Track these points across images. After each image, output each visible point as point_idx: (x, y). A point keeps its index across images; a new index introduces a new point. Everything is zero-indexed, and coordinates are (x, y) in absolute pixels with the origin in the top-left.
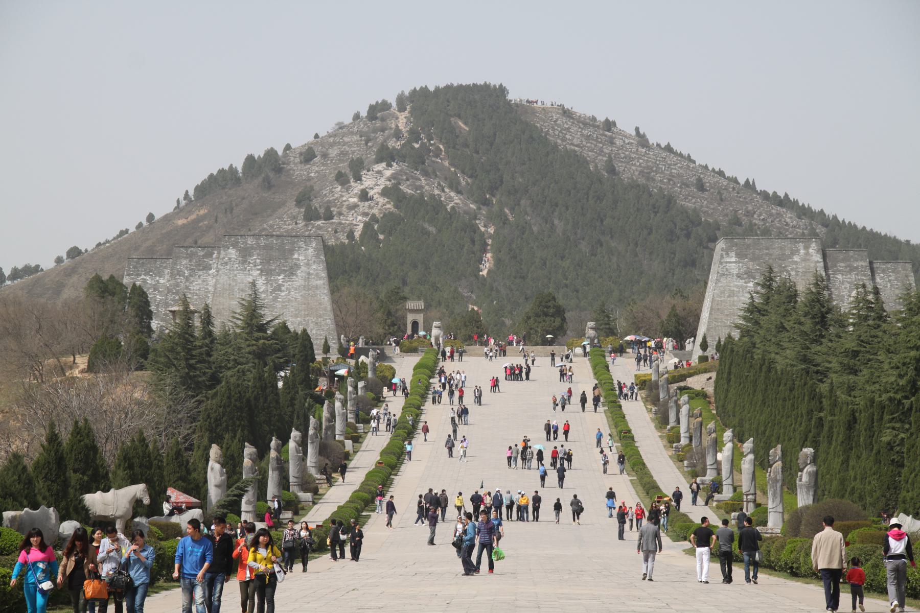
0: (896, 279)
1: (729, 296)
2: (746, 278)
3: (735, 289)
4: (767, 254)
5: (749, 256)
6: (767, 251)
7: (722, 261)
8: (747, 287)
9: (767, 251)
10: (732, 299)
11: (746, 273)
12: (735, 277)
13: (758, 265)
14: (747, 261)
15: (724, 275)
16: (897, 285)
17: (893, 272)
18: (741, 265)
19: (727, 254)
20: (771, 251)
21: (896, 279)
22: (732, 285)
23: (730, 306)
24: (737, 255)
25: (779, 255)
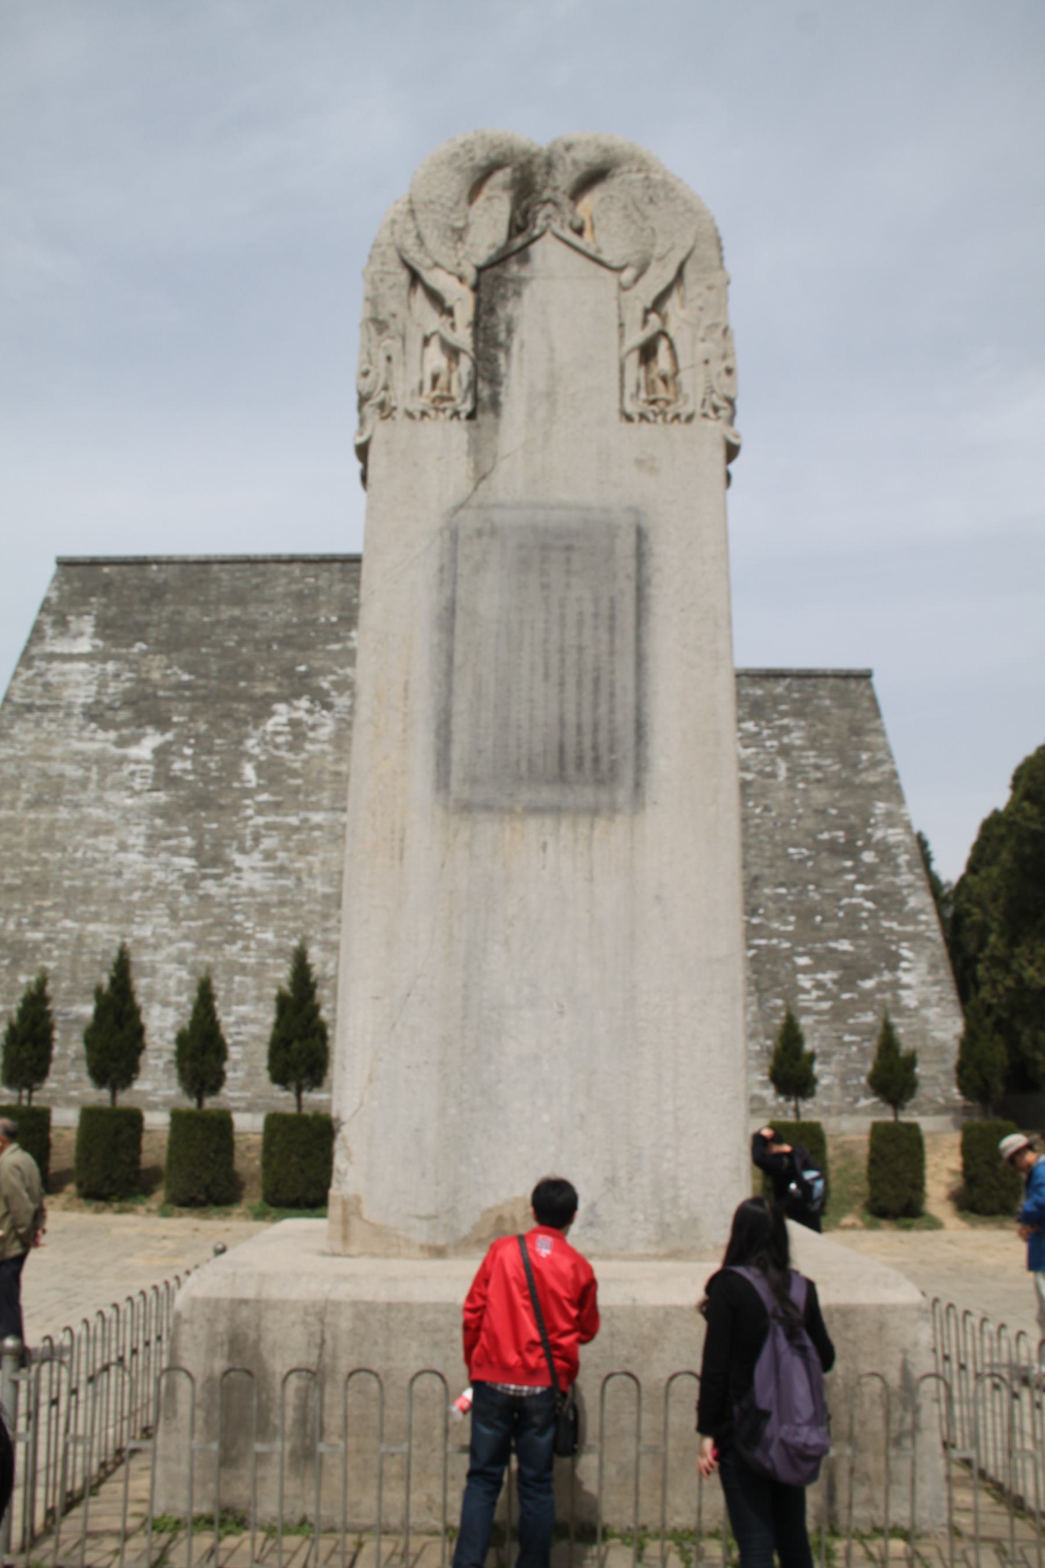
1: (36, 803)
2: (125, 724)
3: (73, 772)
4: (234, 623)
5: (152, 632)
6: (237, 612)
8: (123, 760)
9: (237, 612)
10: (44, 815)
11: (129, 701)
12: (74, 722)
13: (188, 668)
14: (144, 654)
15: (29, 708)
18: (111, 667)
19: (62, 624)
20: (254, 612)
22: (57, 751)
23: (32, 847)
24: (105, 628)
25: (288, 624)
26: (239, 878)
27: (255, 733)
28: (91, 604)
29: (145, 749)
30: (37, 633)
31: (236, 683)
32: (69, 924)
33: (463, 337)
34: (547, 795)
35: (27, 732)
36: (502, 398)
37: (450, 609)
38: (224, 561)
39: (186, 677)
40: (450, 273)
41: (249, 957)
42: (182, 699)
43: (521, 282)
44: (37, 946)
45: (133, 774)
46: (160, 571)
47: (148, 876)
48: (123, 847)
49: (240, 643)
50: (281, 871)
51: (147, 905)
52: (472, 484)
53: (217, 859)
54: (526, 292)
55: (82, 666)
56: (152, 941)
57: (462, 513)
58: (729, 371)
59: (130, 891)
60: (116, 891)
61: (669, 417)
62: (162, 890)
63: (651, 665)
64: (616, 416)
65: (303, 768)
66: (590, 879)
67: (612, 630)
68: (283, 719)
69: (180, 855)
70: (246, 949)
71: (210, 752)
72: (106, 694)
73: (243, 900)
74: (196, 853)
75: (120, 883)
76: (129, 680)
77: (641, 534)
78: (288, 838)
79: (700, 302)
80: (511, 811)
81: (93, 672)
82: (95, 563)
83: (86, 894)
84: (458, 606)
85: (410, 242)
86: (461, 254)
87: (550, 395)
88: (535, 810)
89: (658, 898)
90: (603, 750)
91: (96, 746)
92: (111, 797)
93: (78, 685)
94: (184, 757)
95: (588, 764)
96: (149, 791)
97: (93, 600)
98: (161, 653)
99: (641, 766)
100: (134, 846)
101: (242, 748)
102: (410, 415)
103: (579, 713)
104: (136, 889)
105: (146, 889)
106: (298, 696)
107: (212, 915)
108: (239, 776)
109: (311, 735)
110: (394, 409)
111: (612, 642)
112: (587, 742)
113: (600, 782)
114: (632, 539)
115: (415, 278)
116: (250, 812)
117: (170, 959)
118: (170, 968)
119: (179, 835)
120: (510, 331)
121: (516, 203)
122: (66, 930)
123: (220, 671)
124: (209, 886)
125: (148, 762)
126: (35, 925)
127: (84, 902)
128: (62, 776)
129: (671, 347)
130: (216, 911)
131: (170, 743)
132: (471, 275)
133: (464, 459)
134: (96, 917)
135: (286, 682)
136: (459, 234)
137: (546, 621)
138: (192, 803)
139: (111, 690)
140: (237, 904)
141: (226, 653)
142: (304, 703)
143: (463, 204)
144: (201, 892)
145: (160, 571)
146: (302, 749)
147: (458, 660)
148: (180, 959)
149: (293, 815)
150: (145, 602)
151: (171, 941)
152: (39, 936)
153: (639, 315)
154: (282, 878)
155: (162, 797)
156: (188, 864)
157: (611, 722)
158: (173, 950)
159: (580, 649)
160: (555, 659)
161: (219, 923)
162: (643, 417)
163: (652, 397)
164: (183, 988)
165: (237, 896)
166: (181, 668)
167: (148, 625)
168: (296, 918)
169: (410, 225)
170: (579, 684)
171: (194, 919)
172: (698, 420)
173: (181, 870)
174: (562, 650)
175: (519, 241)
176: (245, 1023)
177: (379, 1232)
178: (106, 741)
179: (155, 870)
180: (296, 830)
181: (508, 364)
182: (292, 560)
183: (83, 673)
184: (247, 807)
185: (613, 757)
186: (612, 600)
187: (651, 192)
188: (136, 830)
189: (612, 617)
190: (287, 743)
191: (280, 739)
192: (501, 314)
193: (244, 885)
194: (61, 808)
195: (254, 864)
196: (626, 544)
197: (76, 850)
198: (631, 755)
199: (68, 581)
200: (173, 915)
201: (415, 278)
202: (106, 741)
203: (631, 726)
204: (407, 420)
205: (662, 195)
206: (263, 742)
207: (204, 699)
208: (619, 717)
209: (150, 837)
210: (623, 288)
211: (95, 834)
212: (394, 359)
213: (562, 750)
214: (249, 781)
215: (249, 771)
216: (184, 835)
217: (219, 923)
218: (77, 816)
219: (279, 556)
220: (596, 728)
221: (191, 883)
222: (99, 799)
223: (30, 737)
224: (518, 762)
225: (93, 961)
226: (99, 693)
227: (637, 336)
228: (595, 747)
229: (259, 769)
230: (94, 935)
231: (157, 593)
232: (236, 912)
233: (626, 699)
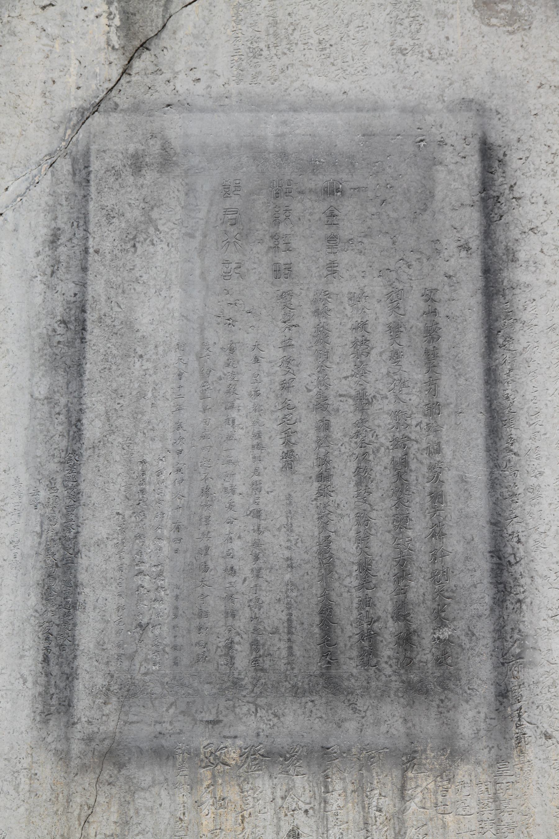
57: (97, 120)
84: (91, 317)
137: (287, 345)
185: (445, 633)
224: (230, 646)
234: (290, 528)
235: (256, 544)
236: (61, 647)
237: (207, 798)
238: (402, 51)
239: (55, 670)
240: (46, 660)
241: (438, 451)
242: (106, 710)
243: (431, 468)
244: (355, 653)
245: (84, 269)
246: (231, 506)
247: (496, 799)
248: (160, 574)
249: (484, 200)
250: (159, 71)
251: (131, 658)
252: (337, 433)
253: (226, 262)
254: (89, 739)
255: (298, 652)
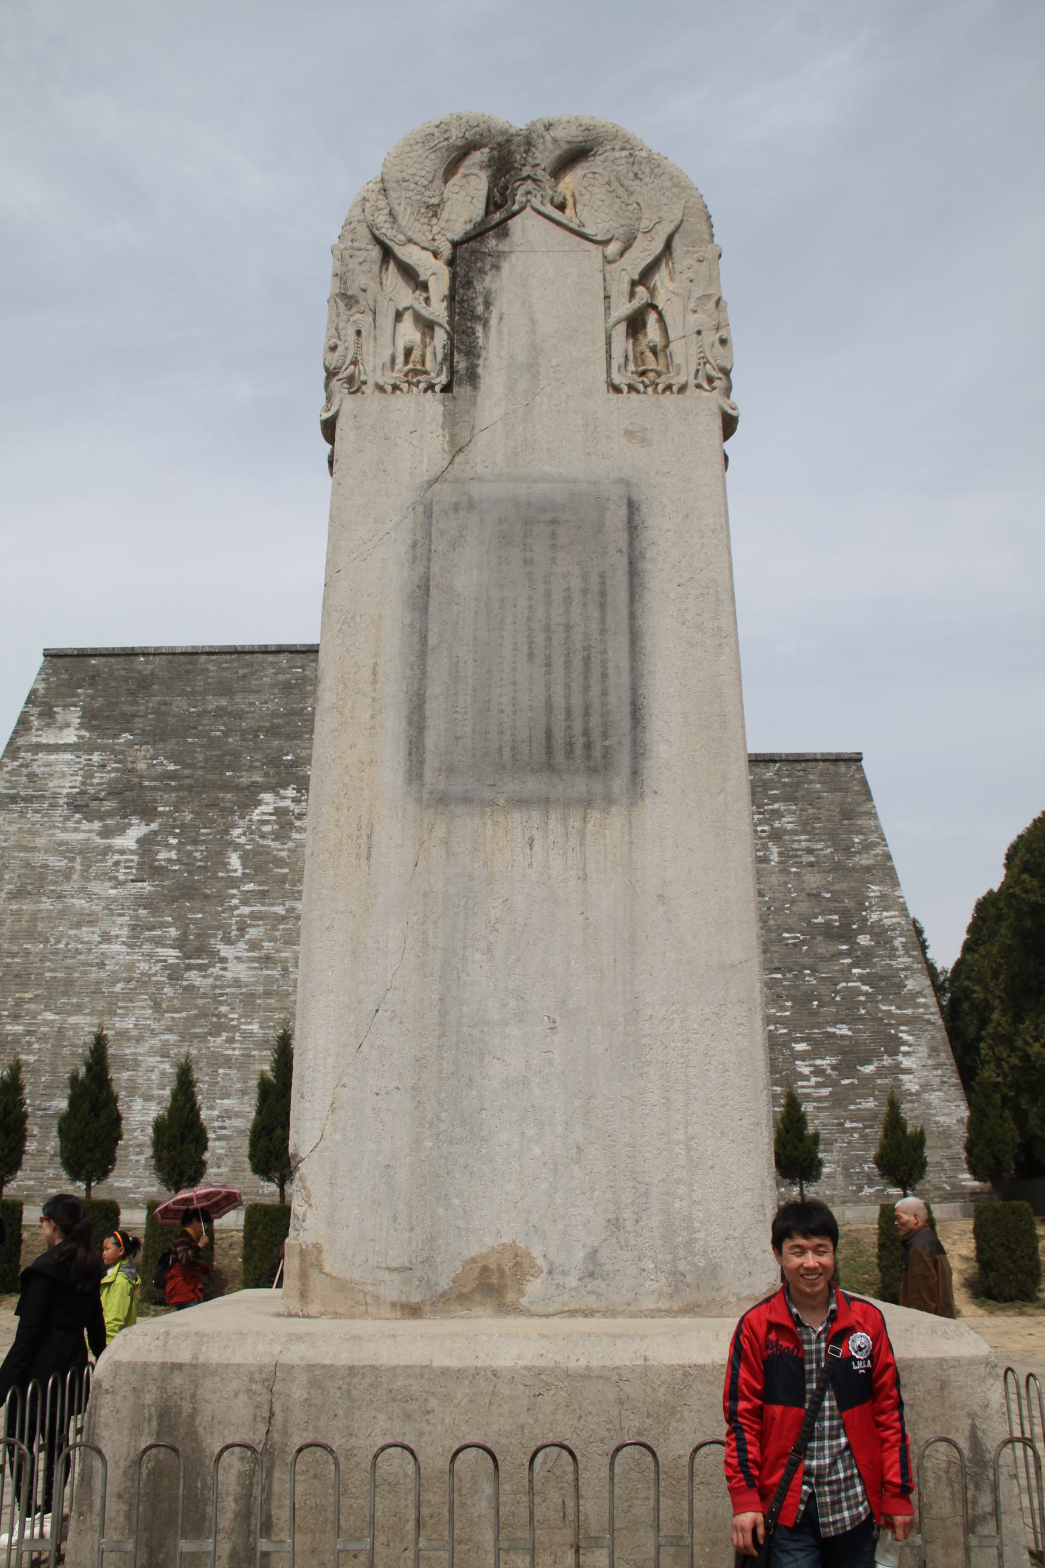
0: (805, 826)
1: (18, 894)
2: (110, 814)
3: (56, 862)
4: (220, 713)
5: (138, 723)
6: (224, 702)
7: (20, 742)
8: (108, 850)
9: (224, 702)
10: (27, 906)
11: (114, 792)
13: (171, 757)
14: (130, 744)
15: (14, 799)
16: (809, 851)
17: (788, 799)
18: (96, 757)
19: (48, 714)
21: (805, 826)
22: (41, 842)
23: (14, 938)
24: (91, 719)
25: (275, 714)
26: (224, 969)
27: (241, 823)
28: (78, 695)
29: (128, 840)
30: (23, 724)
31: (222, 773)
32: (49, 1016)
33: (438, 310)
34: (533, 785)
35: (10, 823)
36: (480, 371)
37: (425, 587)
38: (211, 652)
39: (172, 767)
40: (423, 248)
41: (234, 1049)
42: (167, 789)
43: (500, 255)
44: (16, 1039)
45: (117, 863)
46: (147, 662)
47: (131, 967)
48: (106, 938)
49: (226, 734)
50: (267, 960)
51: (130, 996)
52: (448, 458)
53: (201, 951)
54: (505, 266)
55: (68, 756)
56: (134, 1033)
57: (437, 486)
58: (723, 342)
59: (113, 984)
60: (98, 983)
61: (660, 388)
62: (145, 981)
63: (647, 643)
64: (604, 387)
65: (289, 857)
66: (584, 878)
67: (602, 607)
68: (270, 809)
69: (164, 946)
70: (230, 1040)
71: (195, 842)
72: (92, 785)
73: (228, 990)
74: (180, 944)
75: (103, 975)
76: (114, 770)
77: (632, 507)
78: (274, 928)
79: (690, 275)
80: (493, 803)
81: (79, 763)
82: (83, 654)
83: (68, 985)
84: (432, 584)
85: (382, 219)
86: (435, 230)
87: (532, 367)
88: (520, 802)
89: (661, 897)
90: (596, 735)
91: (81, 836)
92: (95, 887)
93: (63, 775)
94: (169, 847)
95: (579, 751)
96: (133, 881)
97: (80, 691)
98: (147, 743)
99: (638, 752)
100: (117, 936)
101: (228, 837)
102: (381, 389)
103: (567, 696)
104: (119, 981)
105: (128, 980)
106: (285, 786)
107: (197, 1007)
108: (225, 865)
109: (298, 823)
110: (364, 383)
111: (603, 620)
112: (578, 727)
113: (592, 771)
114: (623, 511)
115: (387, 254)
116: (235, 902)
117: (153, 1052)
118: (152, 1060)
119: (163, 925)
120: (488, 304)
121: (494, 181)
122: (46, 1023)
123: (206, 761)
124: (193, 977)
125: (132, 852)
126: (16, 1017)
127: (65, 993)
128: (45, 866)
129: (661, 319)
130: (200, 1002)
131: (155, 833)
132: (446, 249)
133: (440, 432)
134: (78, 1009)
135: (272, 771)
136: (434, 210)
137: (530, 598)
138: (177, 893)
139: (96, 781)
140: (222, 995)
141: (212, 743)
142: (290, 792)
143: (438, 182)
144: (185, 983)
145: (147, 662)
146: (290, 838)
147: (433, 640)
148: (163, 1052)
149: (279, 904)
150: (130, 692)
151: (154, 1033)
152: (19, 1029)
153: (626, 287)
154: (267, 968)
155: (147, 887)
156: (171, 954)
157: (604, 704)
158: (155, 1042)
159: (568, 627)
160: (540, 638)
161: (204, 1014)
162: (631, 388)
163: (641, 369)
164: (166, 1081)
165: (222, 987)
166: (166, 758)
167: (134, 715)
168: (282, 1009)
169: (382, 203)
170: (567, 664)
171: (176, 1011)
172: (691, 391)
173: (165, 961)
174: (547, 629)
175: (497, 217)
176: (229, 1118)
177: (343, 1286)
178: (91, 831)
179: (139, 961)
180: (283, 919)
181: (487, 337)
182: (279, 650)
183: (68, 763)
184: (234, 896)
185: (607, 743)
186: (602, 575)
187: (636, 168)
188: (120, 920)
189: (603, 594)
190: (273, 832)
191: (267, 828)
192: (478, 287)
193: (229, 975)
194: (44, 899)
195: (239, 954)
196: (616, 517)
197: (58, 942)
198: (627, 741)
199: (55, 673)
200: (157, 1006)
201: (387, 254)
202: (91, 831)
203: (627, 709)
204: (377, 393)
205: (647, 171)
206: (249, 831)
207: (190, 788)
208: (613, 699)
209: (133, 928)
210: (607, 261)
211: (79, 925)
212: (364, 333)
213: (549, 735)
214: (236, 871)
215: (235, 861)
216: (169, 925)
217: (204, 1014)
218: (60, 907)
219: (266, 646)
220: (587, 713)
221: (174, 974)
222: (83, 889)
223: (14, 828)
224: (500, 749)
225: (73, 1054)
226: (84, 783)
227: (623, 308)
228: (586, 733)
229: (244, 859)
230: (75, 1027)
231: (144, 684)
232: (221, 1003)
233: (620, 681)
234: (531, 691)
235: (514, 698)
236: (417, 748)
237: (489, 821)
238: (589, 454)
239: (414, 759)
240: (410, 754)
241: (605, 652)
242: (440, 778)
243: (602, 661)
244: (562, 752)
245: (429, 560)
246: (501, 679)
247: (630, 822)
248: (466, 713)
249: (630, 528)
250: (467, 463)
251: (452, 753)
252: (555, 642)
253: (500, 557)
254: (431, 793)
255: (534, 751)
